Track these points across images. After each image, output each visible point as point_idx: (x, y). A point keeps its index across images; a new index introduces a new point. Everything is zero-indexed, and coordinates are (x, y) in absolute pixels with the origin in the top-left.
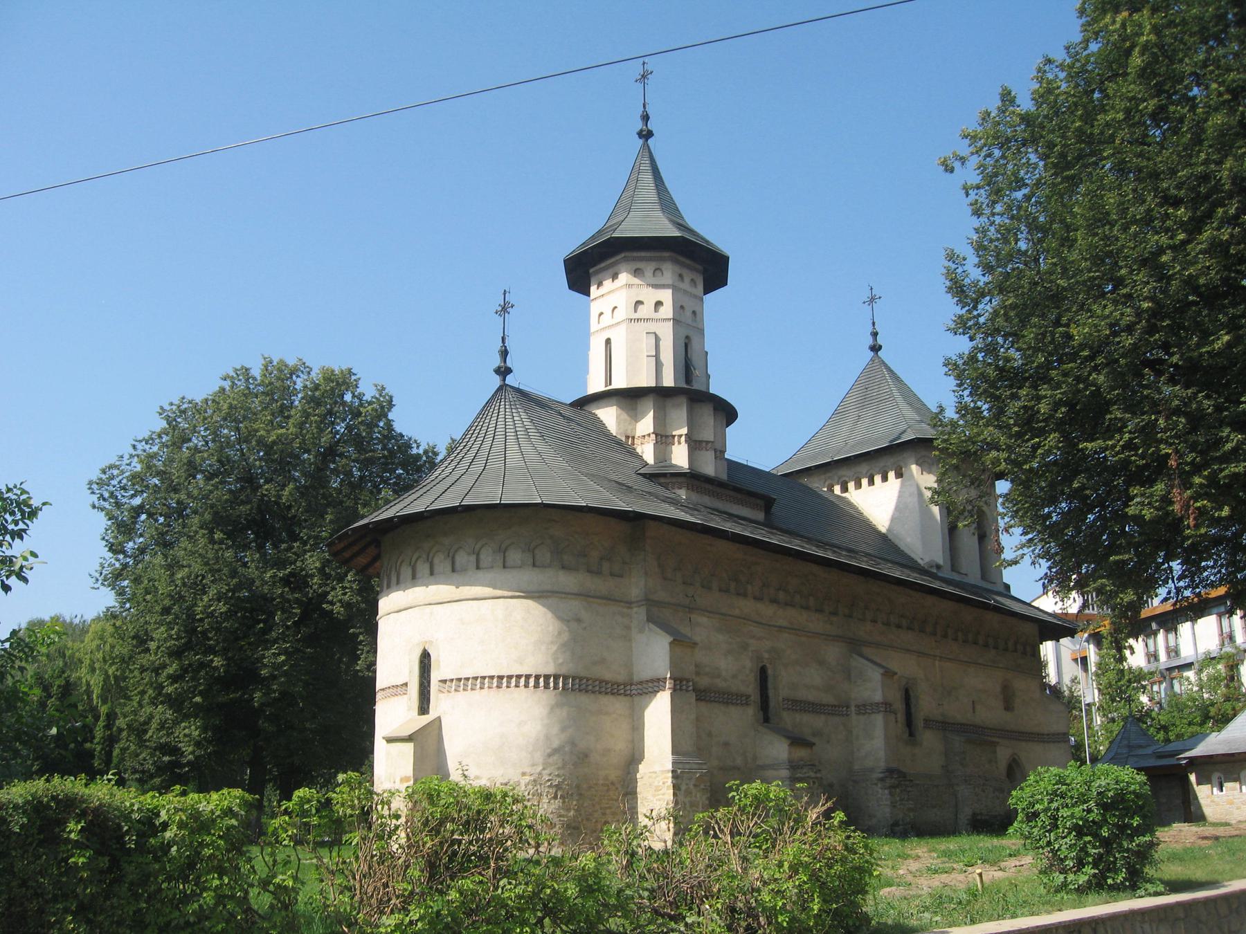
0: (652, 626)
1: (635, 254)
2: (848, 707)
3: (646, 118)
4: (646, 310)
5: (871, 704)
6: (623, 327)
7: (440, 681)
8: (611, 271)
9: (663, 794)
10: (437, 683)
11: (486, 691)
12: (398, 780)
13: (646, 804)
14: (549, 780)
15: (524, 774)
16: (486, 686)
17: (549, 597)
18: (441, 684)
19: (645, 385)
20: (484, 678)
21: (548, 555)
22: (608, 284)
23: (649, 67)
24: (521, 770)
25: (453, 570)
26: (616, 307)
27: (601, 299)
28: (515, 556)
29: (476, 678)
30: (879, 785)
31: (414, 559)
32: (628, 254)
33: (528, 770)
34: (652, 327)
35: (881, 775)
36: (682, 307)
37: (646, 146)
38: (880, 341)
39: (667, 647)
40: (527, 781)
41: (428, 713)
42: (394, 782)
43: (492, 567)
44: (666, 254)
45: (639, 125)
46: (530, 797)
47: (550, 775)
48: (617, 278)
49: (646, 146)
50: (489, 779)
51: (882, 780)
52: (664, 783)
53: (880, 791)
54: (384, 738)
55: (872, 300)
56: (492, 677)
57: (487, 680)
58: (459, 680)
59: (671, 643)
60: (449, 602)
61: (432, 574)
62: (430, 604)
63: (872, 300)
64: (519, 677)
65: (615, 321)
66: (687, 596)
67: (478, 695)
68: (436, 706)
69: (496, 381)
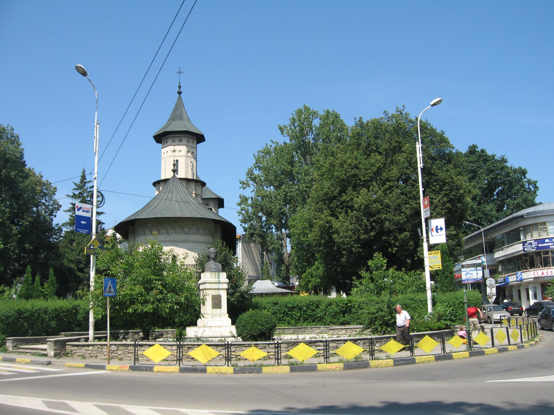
3: (180, 87)
6: (184, 159)
19: (190, 178)
23: (182, 70)
26: (181, 151)
31: (167, 227)
37: (180, 98)
45: (178, 89)
49: (180, 98)
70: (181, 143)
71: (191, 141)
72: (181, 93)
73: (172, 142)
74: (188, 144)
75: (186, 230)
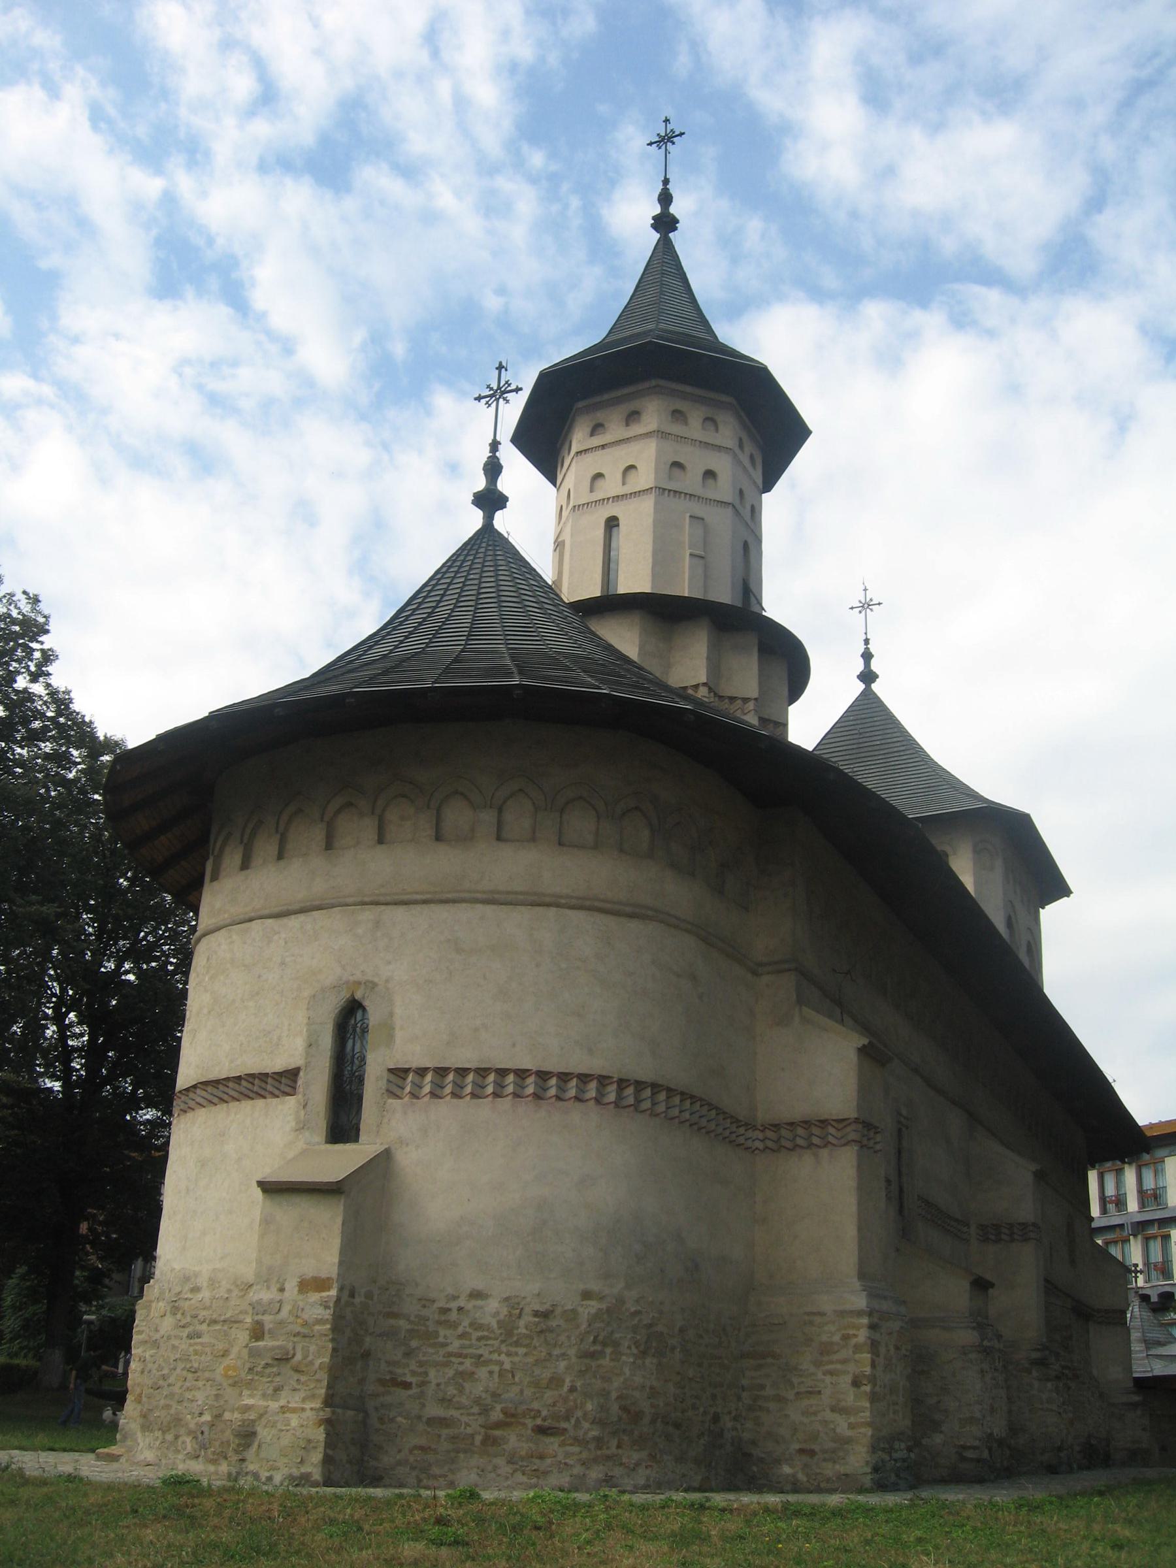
0: (806, 1011)
1: (674, 386)
2: (968, 1225)
4: (691, 481)
5: (1011, 1226)
6: (647, 505)
7: (390, 1071)
8: (625, 408)
9: (844, 1361)
10: (386, 1074)
11: (506, 1103)
12: (291, 1285)
13: (795, 1380)
14: (637, 1313)
15: (587, 1295)
16: (510, 1089)
17: (650, 918)
18: (393, 1078)
20: (502, 1072)
21: (646, 833)
22: (616, 430)
24: (582, 1287)
25: (438, 838)
26: (632, 467)
27: (600, 452)
28: (581, 824)
29: (482, 1072)
30: (1035, 1374)
32: (662, 382)
33: (594, 1286)
34: (699, 509)
35: (1035, 1355)
36: (741, 492)
38: (875, 666)
39: (853, 1056)
40: (593, 1311)
41: (356, 1139)
42: (282, 1290)
43: (533, 839)
44: (725, 398)
46: (598, 1348)
47: (637, 1301)
48: (638, 421)
50: (507, 1299)
51: (1041, 1363)
52: (846, 1338)
53: (1036, 1384)
54: (261, 1184)
55: (866, 606)
56: (521, 1074)
57: (511, 1078)
58: (441, 1072)
59: (863, 1051)
60: (425, 902)
61: (381, 841)
62: (377, 903)
63: (866, 606)
64: (584, 1078)
65: (627, 489)
66: (834, 970)
67: (484, 1111)
68: (379, 1125)
69: (474, 520)
70: (637, 429)
71: (696, 417)
72: (675, 229)
73: (592, 434)
74: (676, 429)
75: (457, 815)
